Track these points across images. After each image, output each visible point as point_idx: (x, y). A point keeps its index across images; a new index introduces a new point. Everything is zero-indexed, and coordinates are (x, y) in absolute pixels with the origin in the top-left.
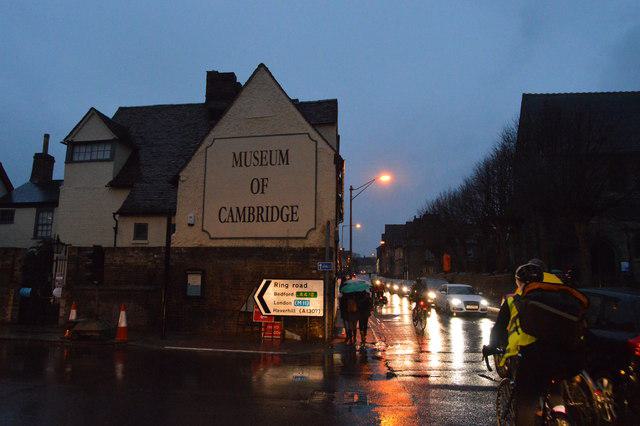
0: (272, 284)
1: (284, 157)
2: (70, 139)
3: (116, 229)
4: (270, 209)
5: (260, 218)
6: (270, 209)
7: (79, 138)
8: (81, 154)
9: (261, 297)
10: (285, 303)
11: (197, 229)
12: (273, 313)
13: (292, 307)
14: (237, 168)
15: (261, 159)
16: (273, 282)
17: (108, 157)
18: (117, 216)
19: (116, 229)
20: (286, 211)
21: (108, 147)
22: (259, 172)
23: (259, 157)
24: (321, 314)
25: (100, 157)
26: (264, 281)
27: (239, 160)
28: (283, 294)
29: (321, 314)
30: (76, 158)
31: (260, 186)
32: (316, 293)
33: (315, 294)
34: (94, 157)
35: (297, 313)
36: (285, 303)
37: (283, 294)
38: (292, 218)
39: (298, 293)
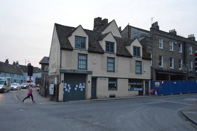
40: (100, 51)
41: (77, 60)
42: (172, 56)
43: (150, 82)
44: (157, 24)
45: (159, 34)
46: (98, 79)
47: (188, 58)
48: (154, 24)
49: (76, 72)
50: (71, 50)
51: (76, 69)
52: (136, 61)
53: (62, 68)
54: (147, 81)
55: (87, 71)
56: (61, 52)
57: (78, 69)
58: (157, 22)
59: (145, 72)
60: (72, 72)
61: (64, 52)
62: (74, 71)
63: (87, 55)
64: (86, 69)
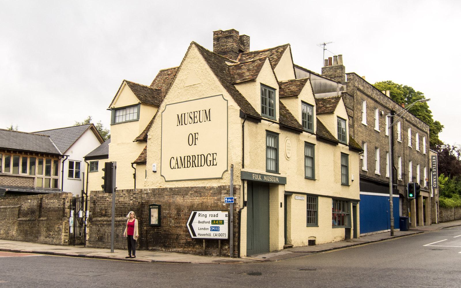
0: (197, 215)
1: (208, 115)
2: (112, 106)
3: (135, 175)
4: (200, 156)
5: (194, 165)
6: (200, 156)
7: (117, 106)
8: (121, 116)
9: (190, 224)
10: (205, 229)
11: (158, 174)
12: (198, 237)
13: (208, 232)
14: (180, 126)
15: (194, 118)
16: (198, 212)
18: (135, 165)
19: (135, 175)
20: (210, 158)
21: (136, 110)
22: (192, 128)
23: (192, 116)
24: (227, 237)
25: (131, 119)
26: (193, 212)
27: (181, 120)
28: (203, 222)
29: (227, 237)
30: (117, 121)
31: (193, 139)
32: (223, 221)
33: (223, 222)
34: (128, 119)
35: (212, 237)
36: (205, 229)
37: (203, 222)
38: (213, 164)
39: (213, 221)
40: (295, 125)
41: (265, 147)
42: (377, 145)
43: (358, 206)
44: (341, 61)
45: (362, 88)
46: (294, 195)
47: (397, 147)
48: (330, 59)
49: (266, 179)
50: (256, 119)
51: (264, 172)
52: (342, 153)
53: (245, 170)
54: (355, 201)
55: (279, 177)
56: (243, 127)
57: (267, 171)
58: (340, 56)
59: (352, 181)
60: (260, 179)
61: (247, 124)
62: (262, 176)
63: (278, 134)
64: (277, 171)
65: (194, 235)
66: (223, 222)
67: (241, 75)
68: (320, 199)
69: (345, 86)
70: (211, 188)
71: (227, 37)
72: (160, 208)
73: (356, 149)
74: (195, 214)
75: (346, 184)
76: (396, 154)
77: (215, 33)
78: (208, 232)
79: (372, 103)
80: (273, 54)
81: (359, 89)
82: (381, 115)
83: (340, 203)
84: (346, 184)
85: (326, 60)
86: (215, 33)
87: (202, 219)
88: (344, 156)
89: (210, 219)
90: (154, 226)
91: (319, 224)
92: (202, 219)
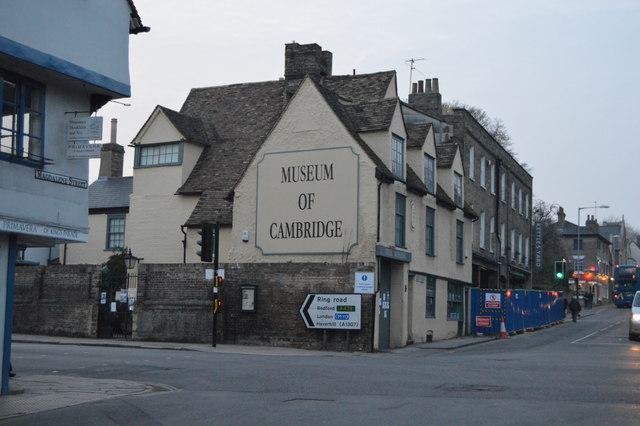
0: (316, 299)
1: (329, 172)
3: (185, 242)
4: (316, 225)
5: (307, 234)
6: (316, 225)
7: (144, 141)
8: (150, 157)
10: (327, 317)
11: (251, 245)
12: (317, 327)
13: (333, 320)
14: (287, 184)
15: (308, 174)
16: (317, 296)
17: (177, 161)
18: (185, 229)
19: (185, 242)
20: (331, 227)
21: (176, 149)
22: (306, 187)
23: (305, 171)
25: (169, 161)
27: (287, 175)
28: (324, 309)
30: (144, 163)
31: (307, 201)
33: (353, 309)
34: (162, 161)
35: (338, 327)
36: (327, 317)
37: (324, 309)
38: (336, 234)
45: (471, 130)
48: (421, 83)
56: (379, 189)
65: (311, 323)
66: (353, 309)
67: (366, 121)
68: (438, 282)
69: (451, 127)
70: (335, 265)
71: (306, 54)
72: (257, 290)
73: (471, 215)
74: (312, 298)
75: (460, 263)
76: (500, 221)
77: (288, 46)
78: (333, 320)
79: (480, 150)
80: (373, 83)
81: (469, 132)
82: (487, 163)
83: (454, 285)
84: (460, 263)
85: (415, 85)
86: (288, 46)
87: (323, 304)
88: (460, 223)
89: (335, 304)
90: (248, 312)
91: (437, 314)
92: (323, 304)
